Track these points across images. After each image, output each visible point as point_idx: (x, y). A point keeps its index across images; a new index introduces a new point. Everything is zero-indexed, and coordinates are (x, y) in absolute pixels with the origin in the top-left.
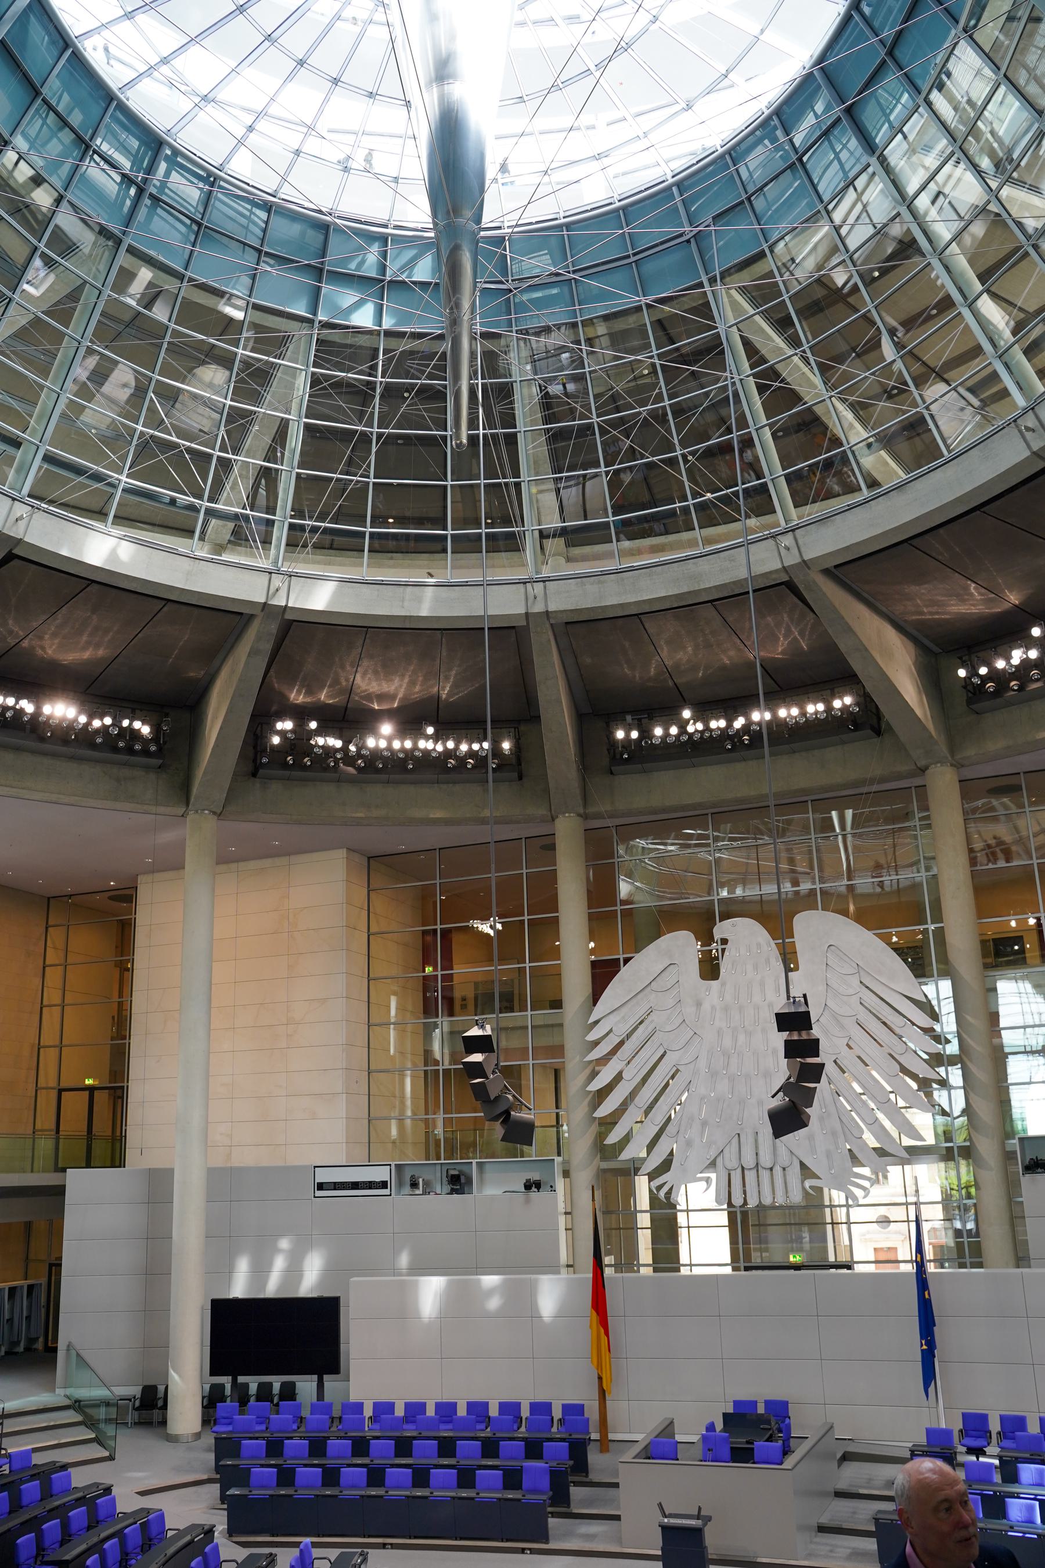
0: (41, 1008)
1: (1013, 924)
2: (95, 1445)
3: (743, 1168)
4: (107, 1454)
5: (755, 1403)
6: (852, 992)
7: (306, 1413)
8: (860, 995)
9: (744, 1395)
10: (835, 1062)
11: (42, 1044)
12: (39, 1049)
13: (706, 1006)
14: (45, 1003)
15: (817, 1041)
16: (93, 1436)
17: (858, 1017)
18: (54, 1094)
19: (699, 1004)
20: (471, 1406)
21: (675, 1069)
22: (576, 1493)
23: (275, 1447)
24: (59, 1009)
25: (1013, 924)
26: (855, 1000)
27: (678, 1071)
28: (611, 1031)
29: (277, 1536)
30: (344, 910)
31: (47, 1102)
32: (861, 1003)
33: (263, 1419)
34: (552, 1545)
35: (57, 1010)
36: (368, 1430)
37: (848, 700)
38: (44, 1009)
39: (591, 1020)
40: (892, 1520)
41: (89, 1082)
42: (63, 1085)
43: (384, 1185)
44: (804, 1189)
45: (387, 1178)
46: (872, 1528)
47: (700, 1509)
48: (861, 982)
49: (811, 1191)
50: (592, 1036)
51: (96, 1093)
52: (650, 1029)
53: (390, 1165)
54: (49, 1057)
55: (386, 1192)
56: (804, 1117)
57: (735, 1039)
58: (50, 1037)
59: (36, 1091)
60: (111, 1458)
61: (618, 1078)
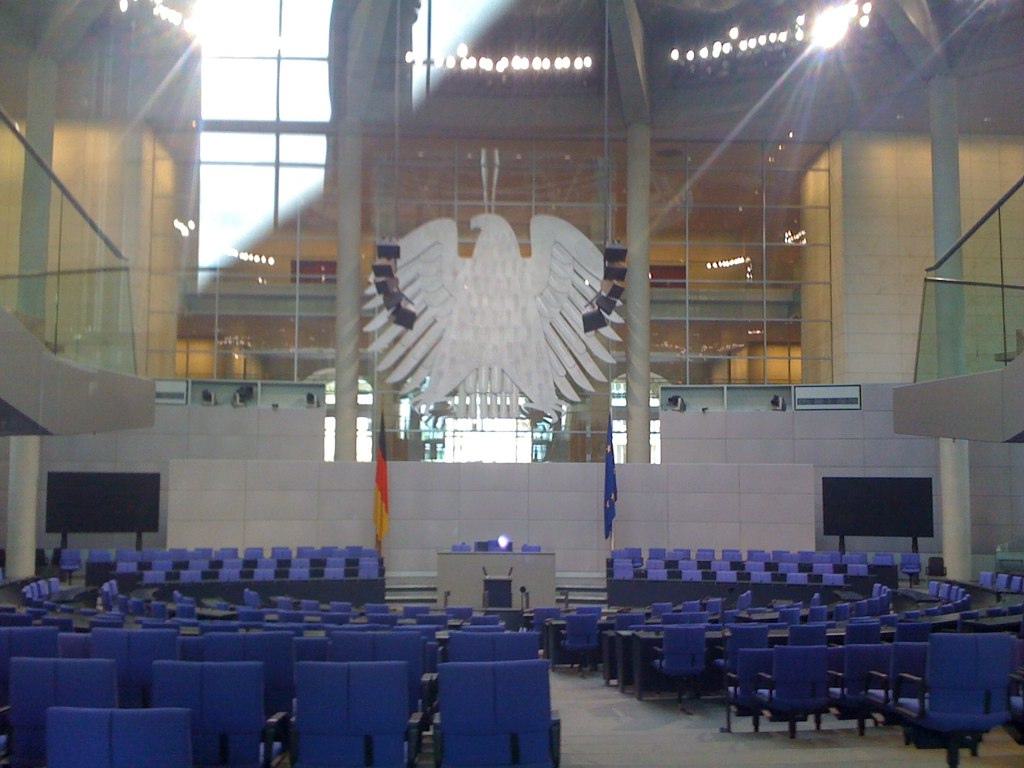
1: (741, 209)
13: (461, 276)
19: (455, 274)
25: (741, 209)
26: (569, 283)
30: (53, 241)
37: (588, 62)
43: (179, 396)
45: (184, 390)
57: (480, 302)
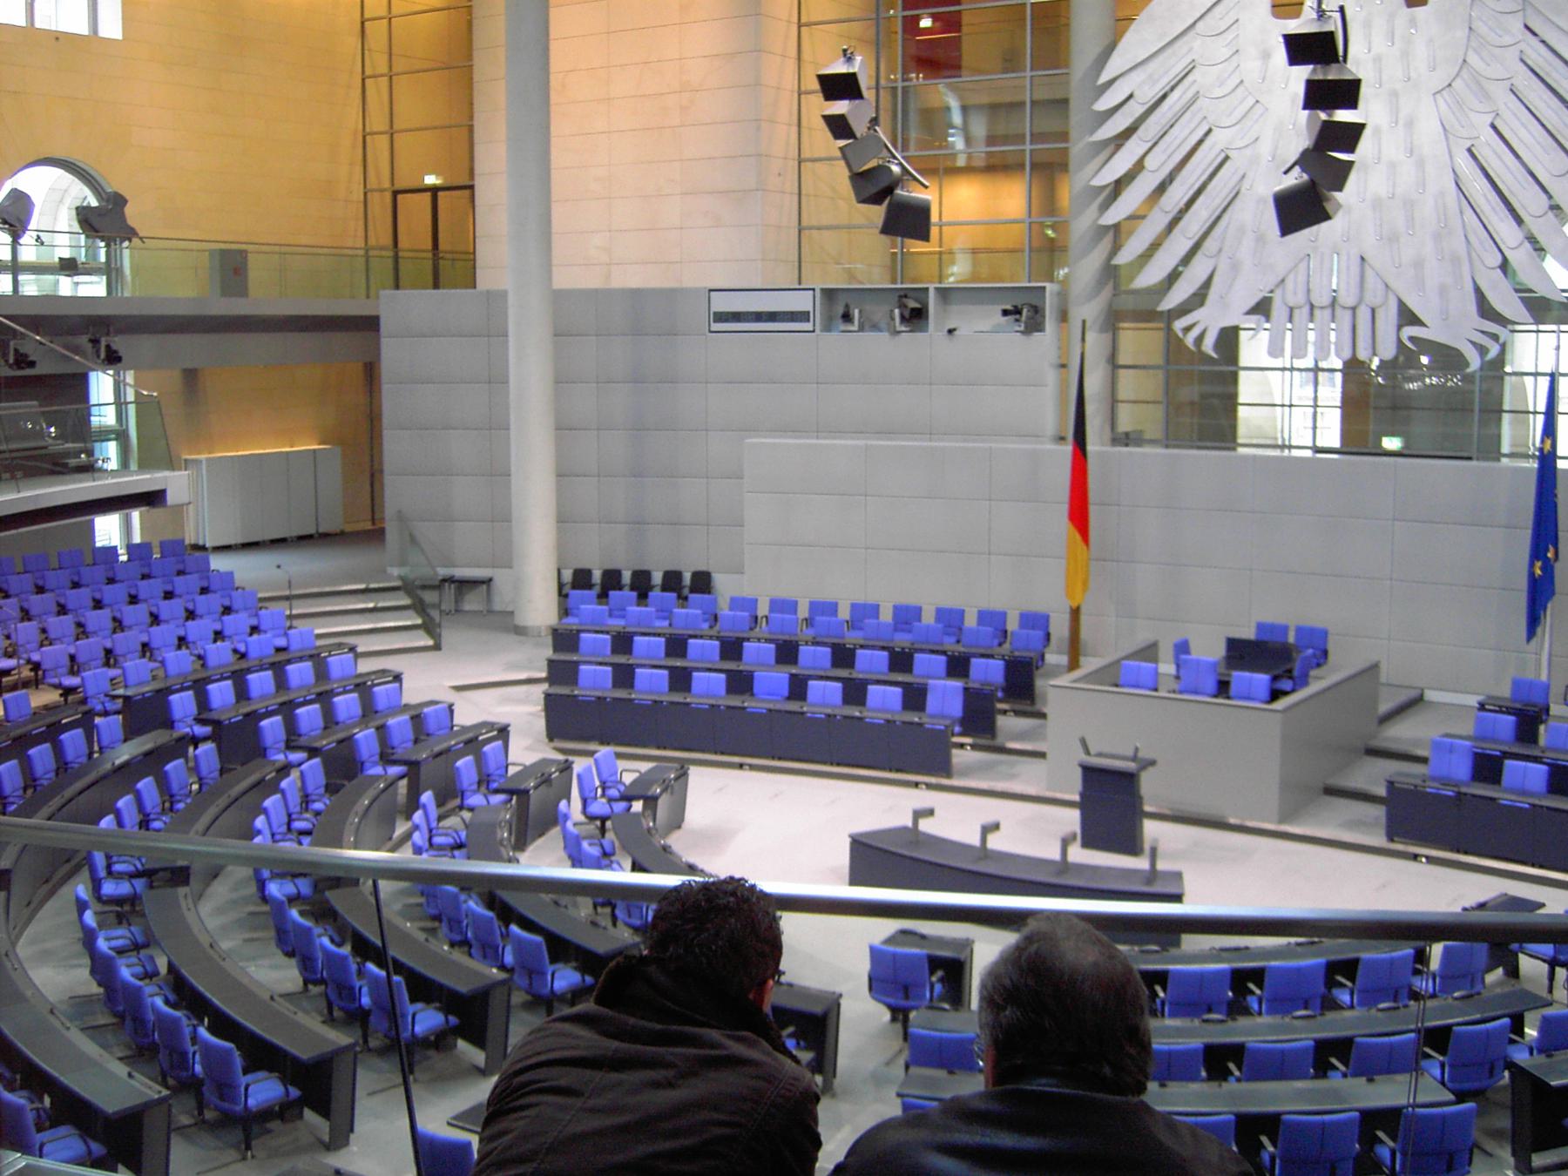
0: (363, 80)
2: (421, 633)
3: (1312, 307)
4: (430, 642)
5: (1285, 629)
6: (1507, 40)
7: (724, 608)
8: (1522, 46)
9: (1270, 617)
10: (1469, 150)
11: (368, 130)
12: (364, 137)
14: (368, 72)
15: (1355, 85)
16: (419, 621)
17: (1513, 81)
18: (388, 197)
20: (941, 614)
21: (1223, 155)
22: (1008, 723)
23: (677, 646)
24: (386, 79)
26: (1511, 56)
27: (1227, 158)
28: (1131, 96)
29: (665, 748)
31: (380, 207)
32: (1522, 61)
33: (665, 613)
34: (955, 782)
35: (384, 81)
36: (851, 638)
38: (367, 81)
39: (1104, 78)
40: (1416, 786)
41: (431, 180)
42: (399, 185)
43: (802, 316)
44: (1399, 341)
45: (808, 307)
46: (1381, 791)
47: (1137, 749)
48: (1527, 27)
49: (1410, 345)
50: (1103, 104)
51: (440, 194)
52: (1190, 94)
53: (814, 290)
54: (380, 145)
55: (808, 326)
56: (1329, 207)
58: (378, 121)
59: (365, 194)
60: (437, 647)
61: (1139, 166)
